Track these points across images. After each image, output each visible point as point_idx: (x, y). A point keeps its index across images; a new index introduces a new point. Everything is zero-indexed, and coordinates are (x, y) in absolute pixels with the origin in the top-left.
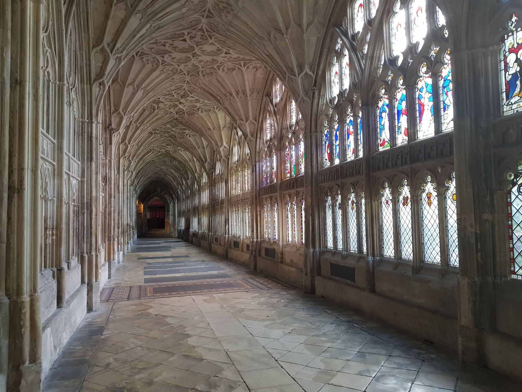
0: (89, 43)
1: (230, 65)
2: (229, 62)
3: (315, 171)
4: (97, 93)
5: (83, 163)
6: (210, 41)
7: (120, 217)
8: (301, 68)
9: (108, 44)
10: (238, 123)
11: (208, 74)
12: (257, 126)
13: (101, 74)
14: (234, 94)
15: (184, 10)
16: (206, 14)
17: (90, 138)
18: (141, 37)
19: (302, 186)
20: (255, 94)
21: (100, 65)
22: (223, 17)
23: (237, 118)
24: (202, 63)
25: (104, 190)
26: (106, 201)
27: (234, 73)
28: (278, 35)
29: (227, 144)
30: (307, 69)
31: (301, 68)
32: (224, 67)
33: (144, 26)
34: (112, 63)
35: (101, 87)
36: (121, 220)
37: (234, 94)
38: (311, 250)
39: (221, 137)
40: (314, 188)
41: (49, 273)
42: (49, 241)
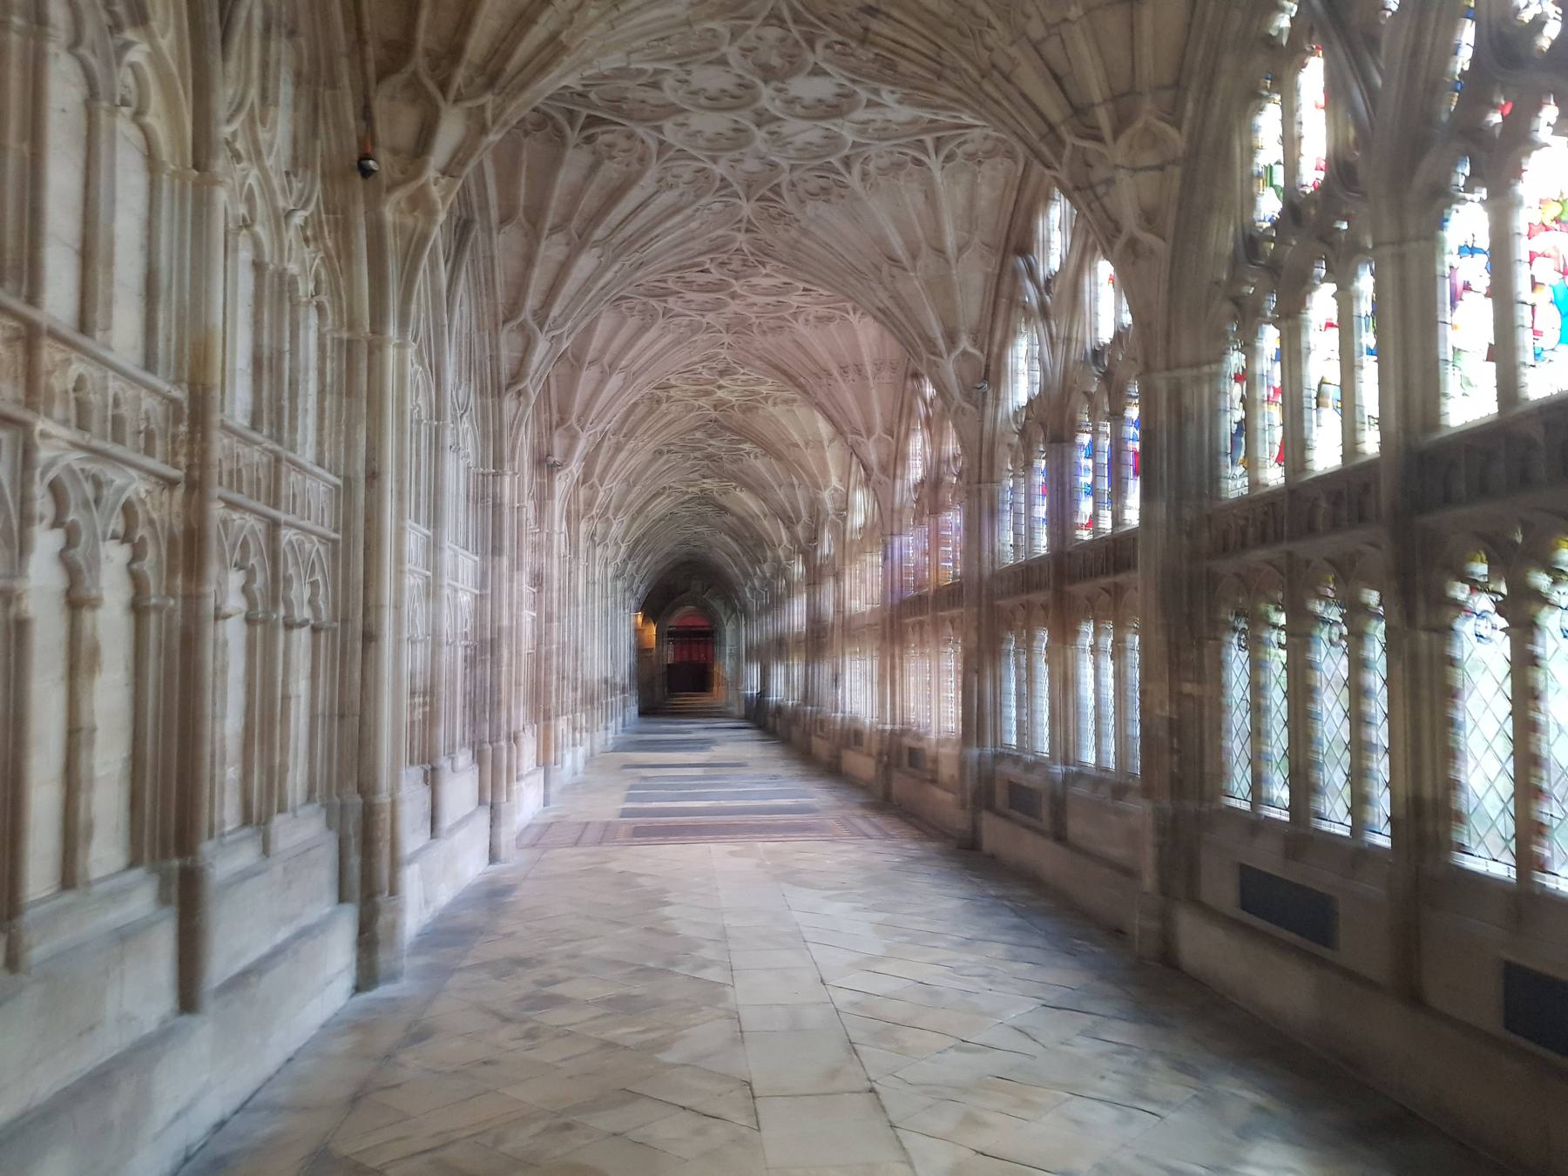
0: (496, 315)
1: (822, 311)
2: (817, 304)
4: (514, 411)
6: (764, 271)
7: (579, 663)
8: (951, 338)
9: (535, 314)
10: (849, 440)
11: (772, 329)
12: (894, 448)
13: (517, 376)
14: (835, 372)
15: (694, 225)
16: (743, 225)
18: (602, 288)
20: (886, 375)
21: (519, 355)
24: (755, 309)
26: (539, 628)
27: (832, 326)
28: (895, 271)
29: (840, 481)
30: (965, 343)
31: (951, 338)
32: (808, 314)
33: (606, 268)
34: (542, 347)
35: (522, 399)
36: (582, 670)
37: (835, 372)
40: (984, 609)
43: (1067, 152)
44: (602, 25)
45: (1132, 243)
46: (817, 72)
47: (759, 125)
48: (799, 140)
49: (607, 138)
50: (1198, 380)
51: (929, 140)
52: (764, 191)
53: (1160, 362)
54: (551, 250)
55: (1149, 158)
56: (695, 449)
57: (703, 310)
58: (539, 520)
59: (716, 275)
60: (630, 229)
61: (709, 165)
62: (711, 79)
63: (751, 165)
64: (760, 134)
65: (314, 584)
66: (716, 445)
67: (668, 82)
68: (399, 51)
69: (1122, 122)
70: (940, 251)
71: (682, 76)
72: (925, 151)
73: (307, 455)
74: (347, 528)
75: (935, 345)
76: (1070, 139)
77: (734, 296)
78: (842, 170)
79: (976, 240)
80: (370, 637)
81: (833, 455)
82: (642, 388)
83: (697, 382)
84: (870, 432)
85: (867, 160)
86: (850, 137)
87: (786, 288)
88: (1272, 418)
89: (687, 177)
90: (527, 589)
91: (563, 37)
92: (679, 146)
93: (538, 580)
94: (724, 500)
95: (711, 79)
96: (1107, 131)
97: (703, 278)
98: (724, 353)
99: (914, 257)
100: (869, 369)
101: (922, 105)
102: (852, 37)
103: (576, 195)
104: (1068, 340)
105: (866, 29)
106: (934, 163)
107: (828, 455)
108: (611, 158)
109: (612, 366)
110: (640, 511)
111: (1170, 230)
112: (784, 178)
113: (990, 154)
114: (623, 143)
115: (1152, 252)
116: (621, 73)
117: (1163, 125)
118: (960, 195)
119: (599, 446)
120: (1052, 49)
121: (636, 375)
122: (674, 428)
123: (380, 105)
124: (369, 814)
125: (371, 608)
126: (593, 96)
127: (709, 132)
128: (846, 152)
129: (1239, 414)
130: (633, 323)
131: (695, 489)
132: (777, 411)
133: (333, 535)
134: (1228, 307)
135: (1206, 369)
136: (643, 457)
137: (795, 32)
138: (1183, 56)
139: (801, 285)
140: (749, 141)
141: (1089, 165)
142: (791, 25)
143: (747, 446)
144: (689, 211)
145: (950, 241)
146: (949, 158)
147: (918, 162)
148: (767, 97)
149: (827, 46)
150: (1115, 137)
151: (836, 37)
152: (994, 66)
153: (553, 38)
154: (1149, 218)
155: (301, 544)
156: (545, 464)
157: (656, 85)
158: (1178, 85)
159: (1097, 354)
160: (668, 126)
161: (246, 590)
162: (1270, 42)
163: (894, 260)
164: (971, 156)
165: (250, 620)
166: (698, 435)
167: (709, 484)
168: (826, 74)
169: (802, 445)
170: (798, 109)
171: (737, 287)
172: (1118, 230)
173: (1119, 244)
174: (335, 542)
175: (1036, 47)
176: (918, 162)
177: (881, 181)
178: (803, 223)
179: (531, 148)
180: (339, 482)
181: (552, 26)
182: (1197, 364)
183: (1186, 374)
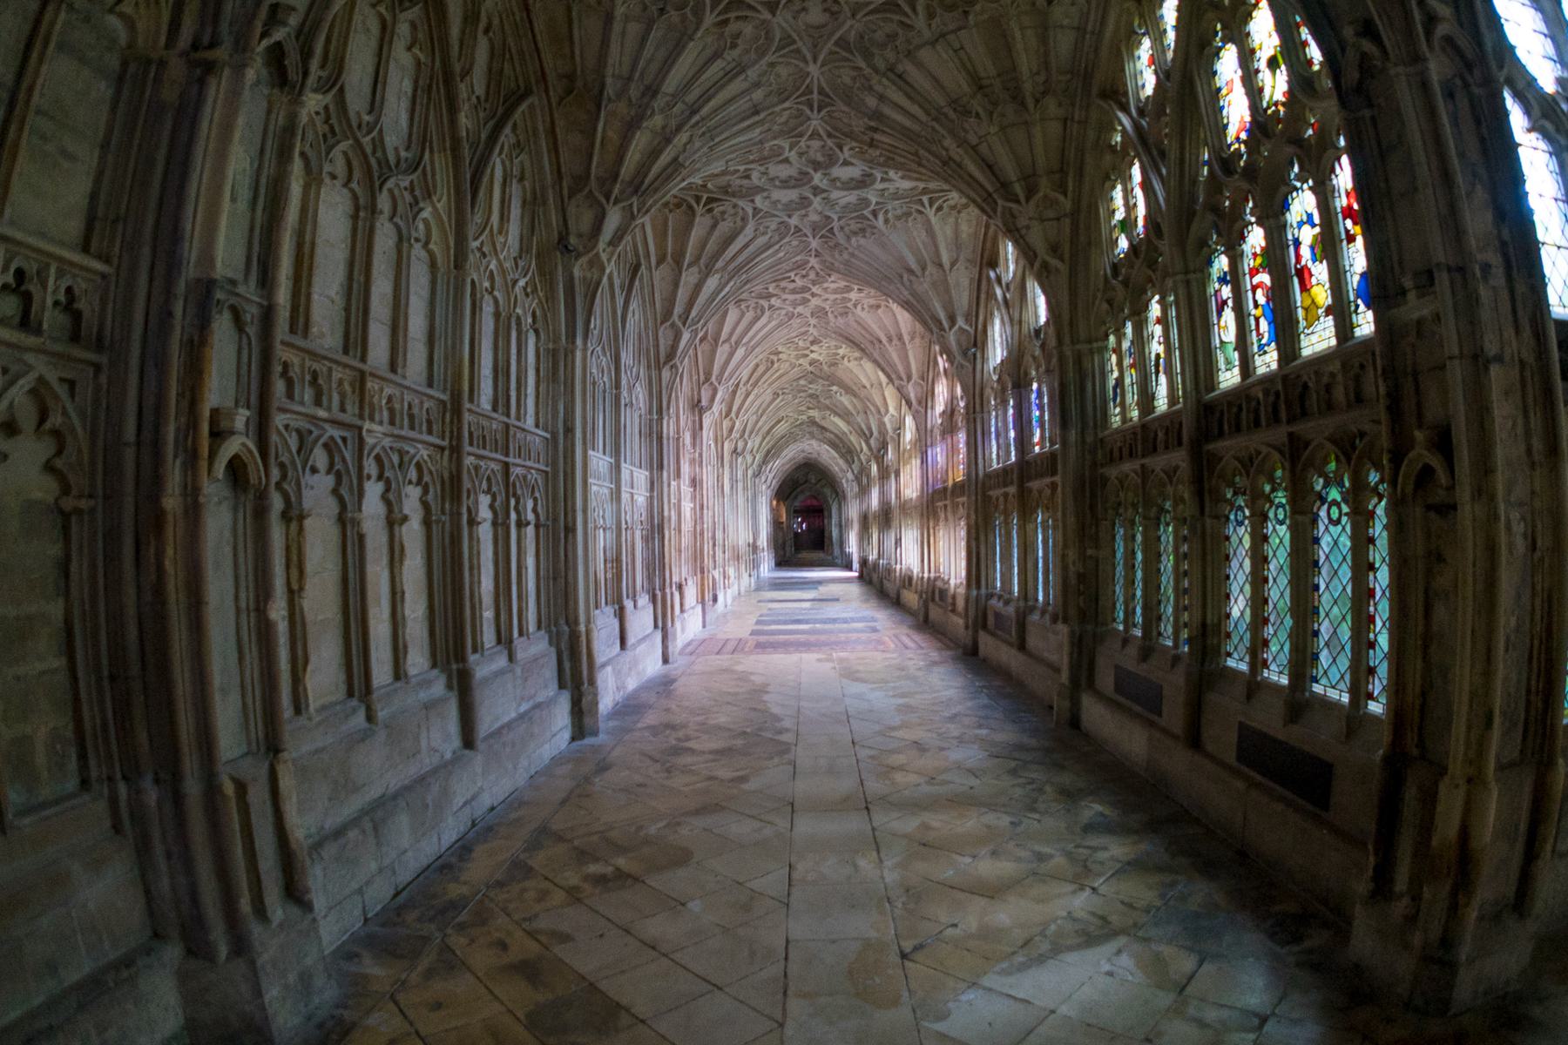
0: (656, 320)
1: (872, 301)
3: (981, 473)
5: (651, 473)
9: (680, 317)
13: (671, 355)
14: (884, 340)
15: (781, 254)
16: (813, 253)
17: (660, 438)
19: (962, 494)
20: (917, 340)
22: (837, 256)
23: (893, 376)
25: (694, 498)
27: (880, 311)
34: (686, 336)
37: (884, 340)
38: (974, 593)
39: (885, 399)
41: (609, 610)
42: (609, 575)
43: (999, 209)
44: (705, 149)
45: (1045, 266)
46: (846, 163)
47: (815, 195)
48: (843, 202)
49: (721, 208)
50: (1091, 352)
51: (925, 199)
52: (823, 232)
53: (1067, 340)
54: (689, 277)
55: (1051, 214)
56: (800, 391)
57: (795, 304)
58: (694, 445)
59: (799, 283)
60: (740, 259)
61: (786, 219)
62: (784, 172)
63: (814, 217)
64: (817, 202)
65: (535, 500)
66: (816, 388)
67: (755, 175)
68: (581, 180)
69: (1031, 192)
70: (940, 265)
71: (762, 169)
72: (924, 206)
73: (530, 422)
74: (554, 464)
75: (941, 324)
76: (1000, 202)
77: (813, 295)
78: (871, 217)
79: (962, 257)
80: (570, 530)
81: (890, 394)
82: (760, 355)
83: (797, 349)
84: (909, 378)
85: (886, 212)
86: (874, 200)
87: (848, 289)
88: (1130, 377)
89: (773, 226)
90: (686, 489)
91: (681, 159)
92: (765, 209)
93: (694, 483)
94: (823, 423)
95: (784, 172)
96: (1022, 199)
97: (792, 286)
98: (811, 330)
99: (924, 269)
100: (906, 338)
101: (917, 179)
102: (861, 142)
103: (703, 245)
104: (1020, 322)
105: (872, 139)
106: (930, 212)
107: (886, 393)
108: (724, 220)
109: (737, 343)
110: (768, 432)
111: (1067, 256)
112: (836, 225)
113: (966, 206)
114: (732, 211)
115: (1057, 270)
116: (724, 173)
117: (1057, 195)
118: (949, 231)
119: (734, 392)
120: (984, 149)
121: (753, 348)
122: (784, 379)
123: (572, 210)
124: (574, 637)
125: (570, 511)
126: (709, 185)
127: (785, 200)
128: (872, 207)
129: (1116, 374)
130: (749, 315)
131: (804, 417)
132: (853, 365)
133: (544, 468)
134: (1105, 306)
135: (1095, 345)
136: (768, 397)
137: (830, 142)
138: (1063, 155)
139: (856, 287)
140: (810, 204)
141: (1013, 216)
142: (825, 137)
143: (835, 388)
144: (777, 247)
145: (946, 259)
146: (940, 209)
147: (920, 212)
148: (818, 179)
149: (851, 149)
150: (1028, 200)
151: (854, 144)
152: (950, 158)
153: (675, 159)
154: (1054, 249)
155: (525, 477)
156: (697, 408)
157: (748, 177)
158: (1063, 171)
159: (1037, 332)
160: (758, 199)
161: (492, 507)
162: (1112, 149)
163: (911, 271)
164: (953, 208)
165: (495, 524)
166: (802, 382)
167: (812, 413)
168: (852, 164)
169: (868, 386)
170: (838, 184)
171: (814, 289)
172: (1036, 255)
173: (1037, 265)
174: (546, 472)
175: (974, 148)
176: (920, 212)
177: (898, 224)
178: (851, 250)
179: (673, 219)
180: (548, 436)
181: (673, 154)
182: (1090, 342)
183: (1083, 347)
